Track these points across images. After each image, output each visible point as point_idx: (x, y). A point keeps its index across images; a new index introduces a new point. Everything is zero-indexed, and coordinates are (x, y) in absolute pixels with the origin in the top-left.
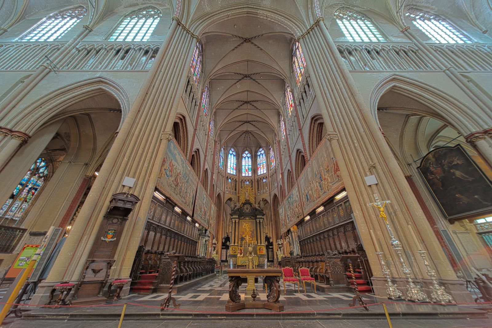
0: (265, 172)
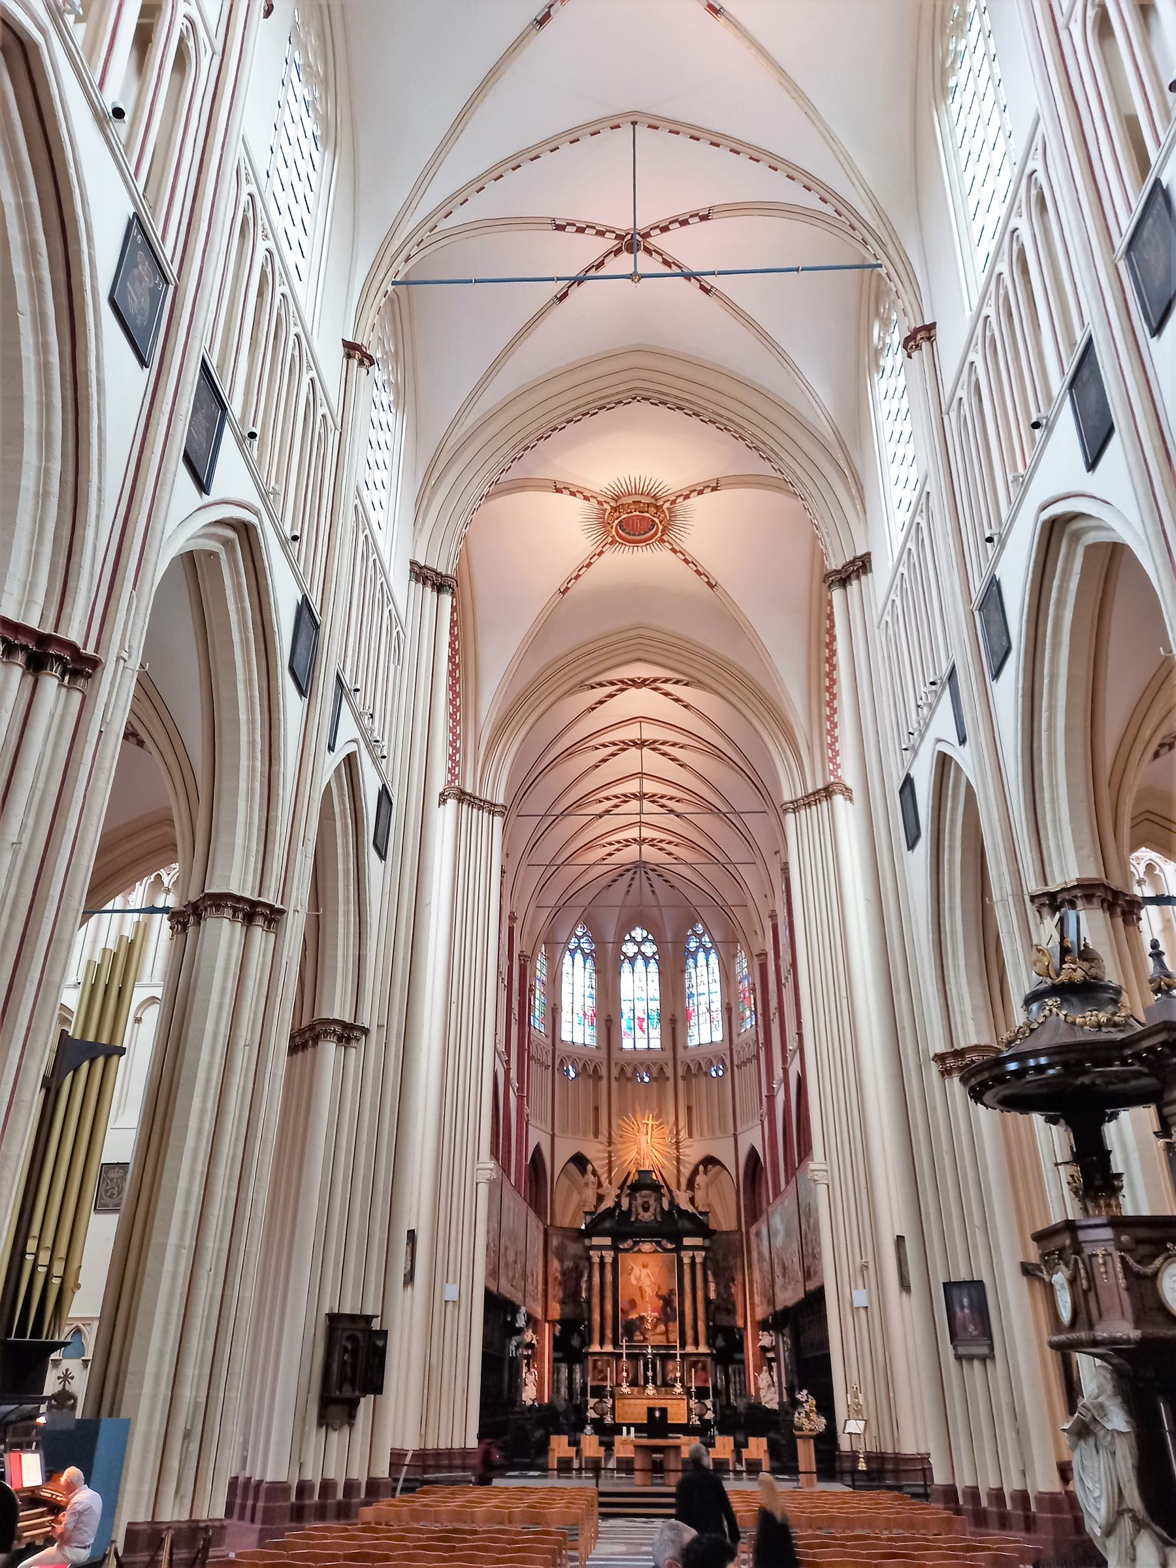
0: (718, 1036)
